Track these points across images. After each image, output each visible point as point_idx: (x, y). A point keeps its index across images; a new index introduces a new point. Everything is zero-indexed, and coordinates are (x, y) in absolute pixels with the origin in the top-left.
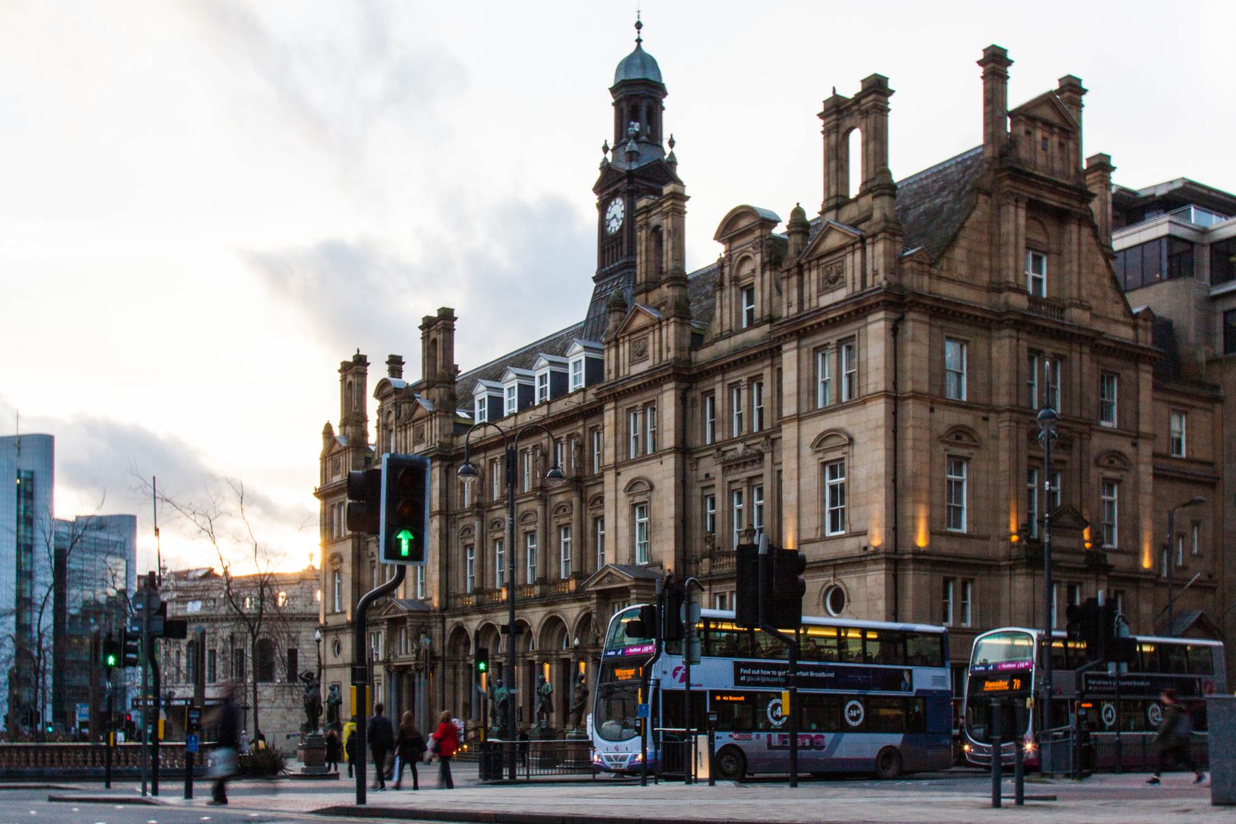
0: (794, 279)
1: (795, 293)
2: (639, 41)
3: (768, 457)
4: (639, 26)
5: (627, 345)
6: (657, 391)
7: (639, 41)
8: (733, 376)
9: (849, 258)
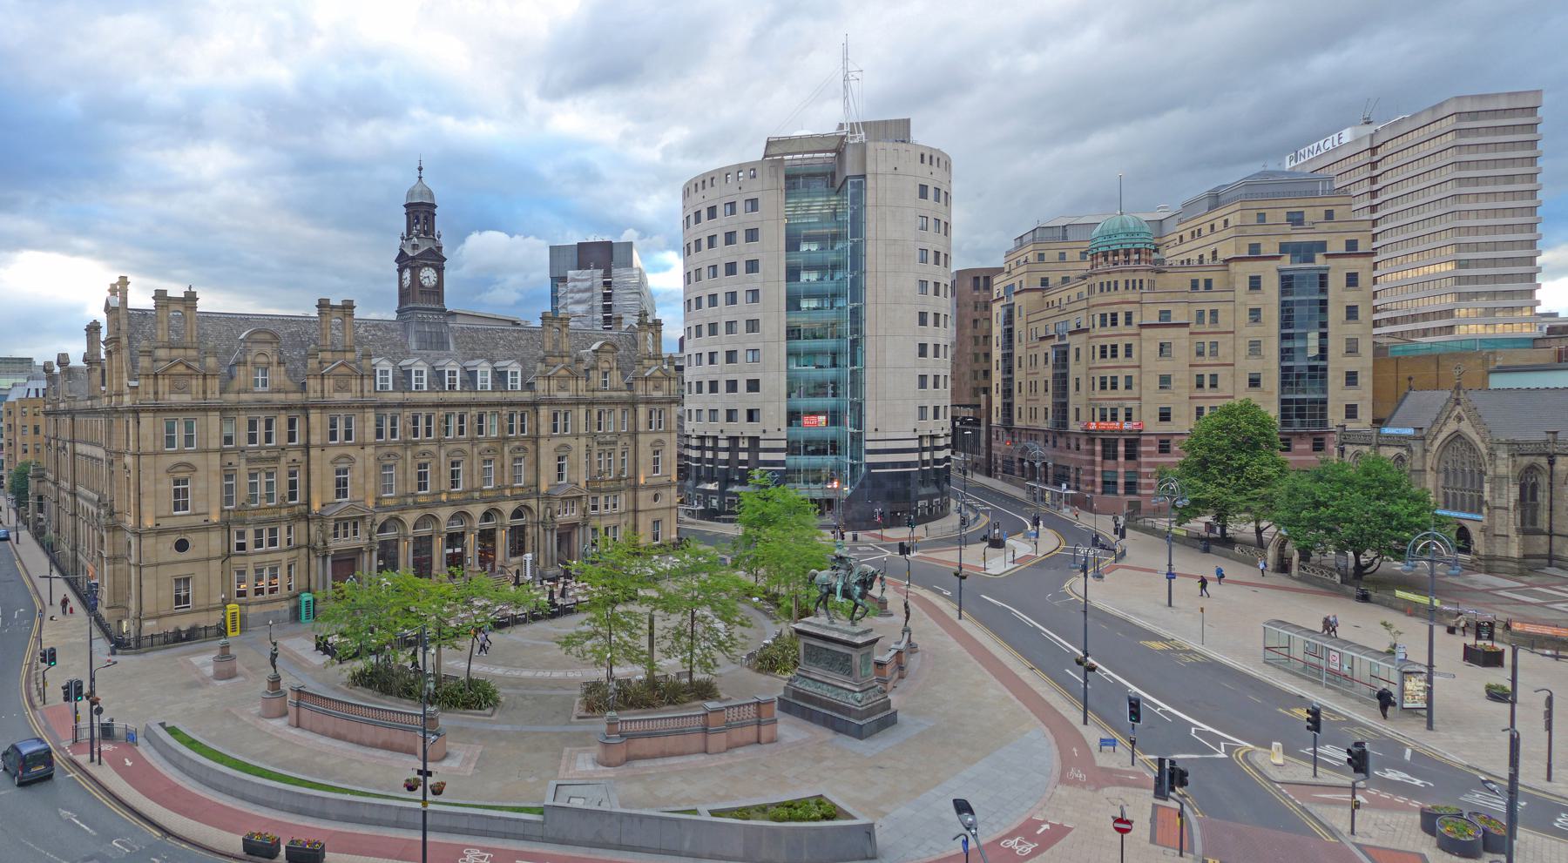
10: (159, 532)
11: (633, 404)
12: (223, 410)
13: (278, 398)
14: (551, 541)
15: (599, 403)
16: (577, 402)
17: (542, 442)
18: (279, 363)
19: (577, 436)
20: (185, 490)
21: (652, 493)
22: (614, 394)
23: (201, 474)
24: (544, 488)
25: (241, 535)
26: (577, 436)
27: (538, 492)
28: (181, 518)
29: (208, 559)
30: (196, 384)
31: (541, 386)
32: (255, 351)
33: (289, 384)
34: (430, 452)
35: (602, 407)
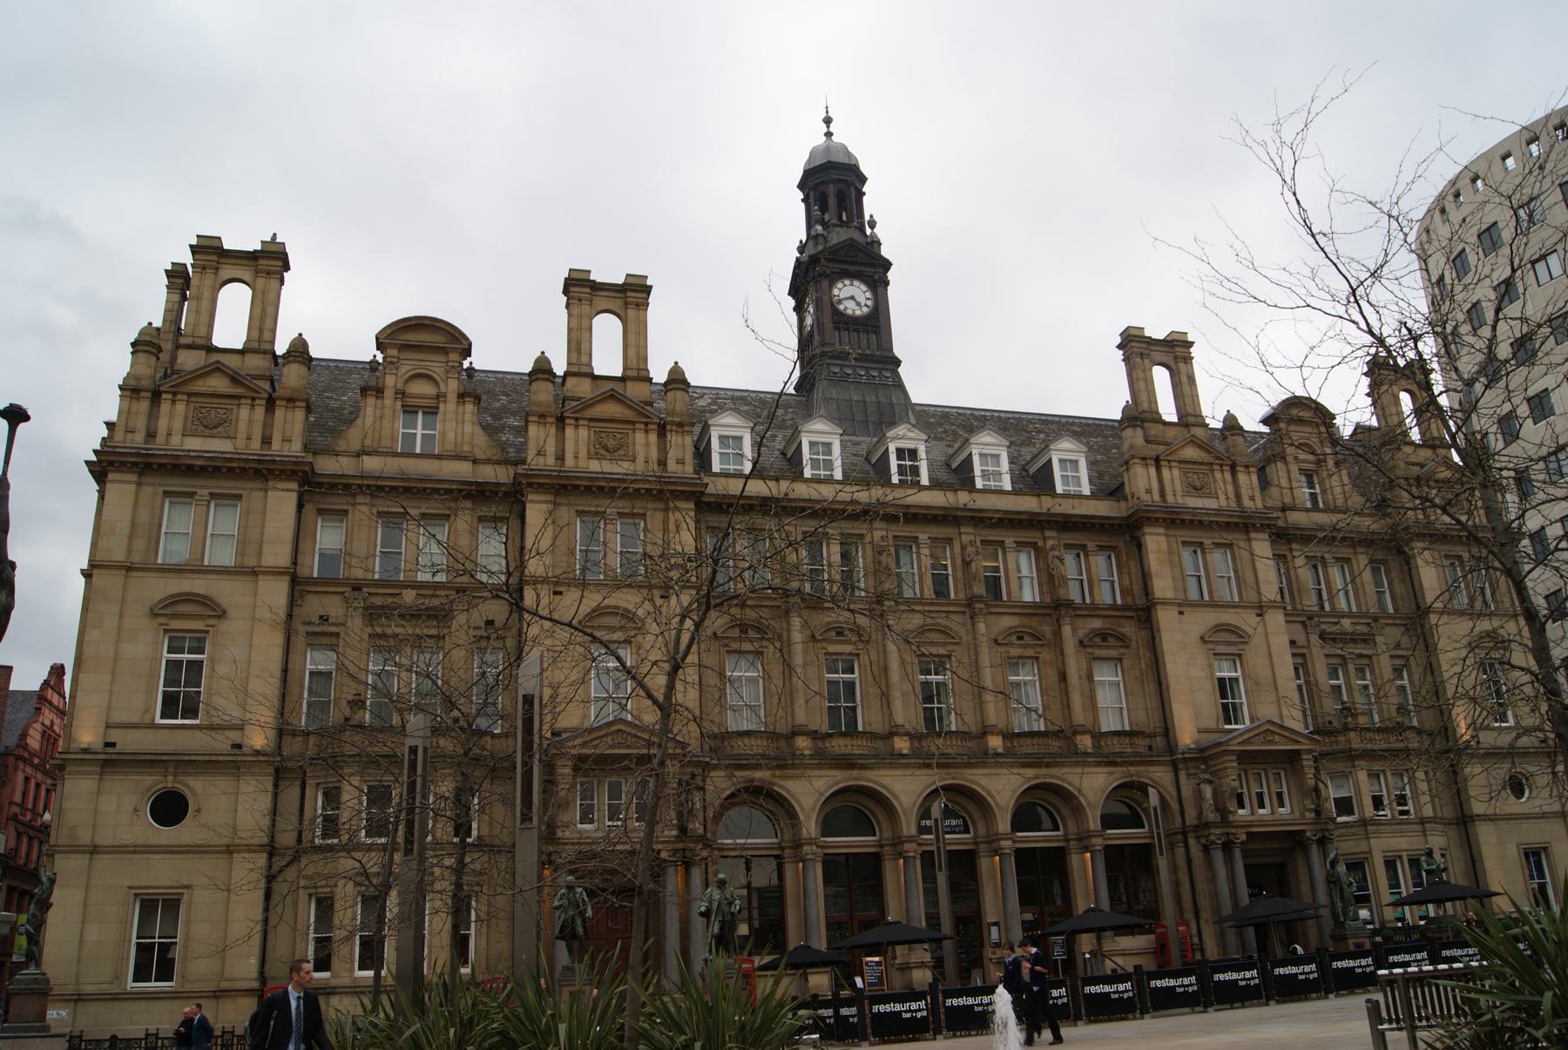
5: (1176, 472)
8: (1314, 550)
10: (110, 761)
14: (1228, 883)
17: (1165, 618)
18: (462, 397)
19: (1261, 609)
21: (1502, 770)
23: (234, 627)
24: (1186, 735)
25: (332, 797)
27: (1171, 747)
28: (181, 736)
29: (229, 850)
30: (248, 417)
32: (406, 369)
33: (480, 443)
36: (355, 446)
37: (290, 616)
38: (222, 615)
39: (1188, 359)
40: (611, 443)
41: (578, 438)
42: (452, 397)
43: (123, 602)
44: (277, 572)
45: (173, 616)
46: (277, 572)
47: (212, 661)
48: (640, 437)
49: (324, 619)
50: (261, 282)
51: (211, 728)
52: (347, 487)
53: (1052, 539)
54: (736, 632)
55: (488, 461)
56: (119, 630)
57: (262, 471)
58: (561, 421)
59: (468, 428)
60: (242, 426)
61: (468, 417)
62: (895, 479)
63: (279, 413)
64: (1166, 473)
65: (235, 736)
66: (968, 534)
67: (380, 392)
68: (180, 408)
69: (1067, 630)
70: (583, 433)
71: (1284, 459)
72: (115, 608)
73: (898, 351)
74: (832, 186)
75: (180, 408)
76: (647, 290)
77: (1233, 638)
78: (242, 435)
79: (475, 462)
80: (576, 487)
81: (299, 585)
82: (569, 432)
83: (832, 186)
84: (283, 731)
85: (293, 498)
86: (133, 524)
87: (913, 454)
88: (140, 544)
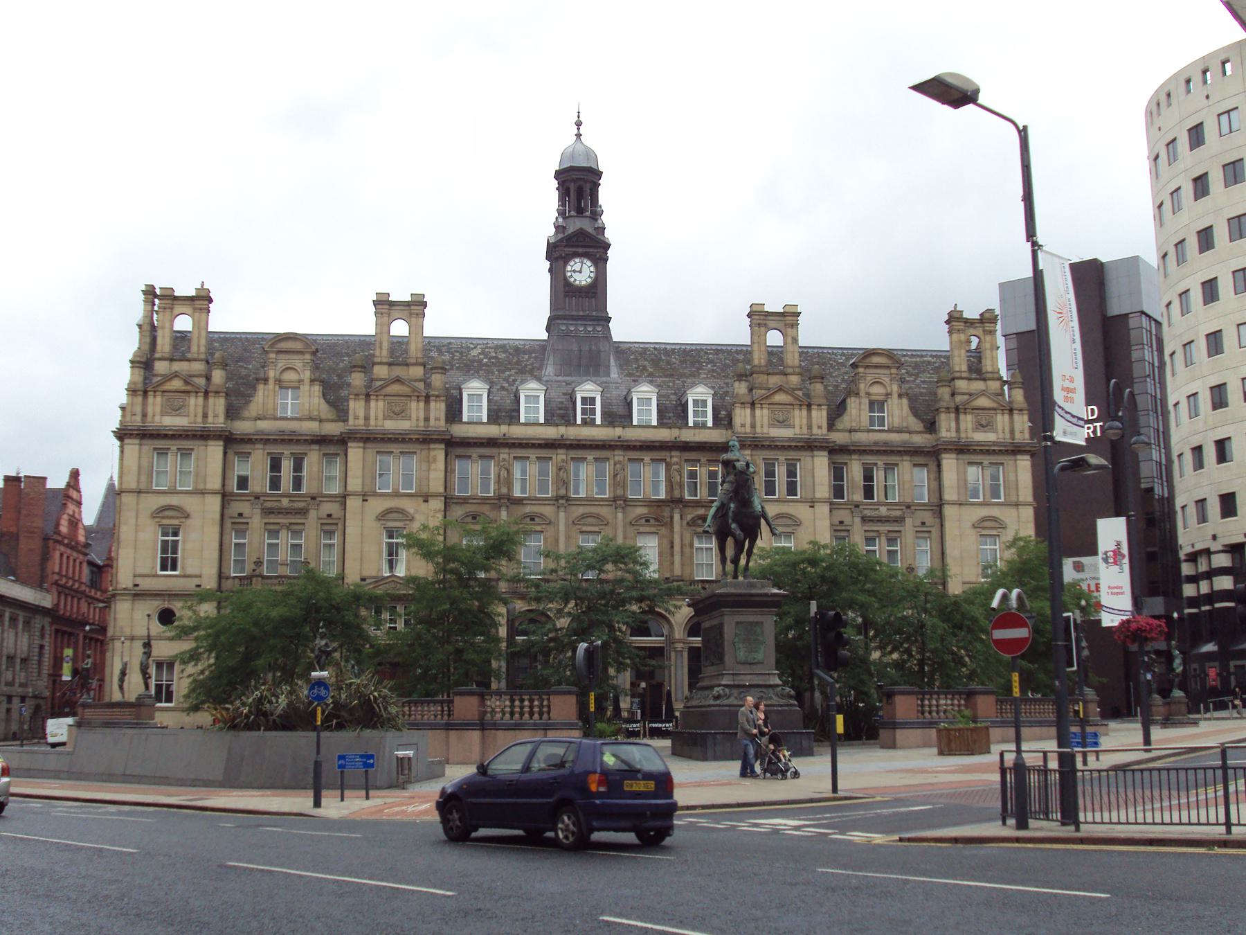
0: (953, 415)
1: (953, 424)
2: (579, 135)
3: (909, 521)
4: (579, 124)
5: (765, 411)
6: (808, 453)
7: (579, 135)
9: (999, 417)
10: (138, 595)
11: (931, 456)
12: (230, 441)
13: (311, 427)
15: (861, 451)
16: (810, 446)
18: (312, 381)
19: (812, 503)
20: (175, 543)
22: (894, 437)
26: (812, 503)
30: (195, 403)
31: (742, 417)
32: (281, 364)
34: (541, 516)
35: (870, 459)
36: (254, 414)
37: (222, 515)
38: (188, 516)
39: (795, 325)
40: (397, 409)
41: (378, 407)
42: (307, 381)
43: (137, 511)
44: (214, 493)
45: (163, 518)
46: (214, 493)
47: (184, 542)
48: (414, 405)
49: (241, 515)
50: (197, 315)
51: (185, 576)
52: (250, 440)
53: (676, 457)
54: (469, 519)
55: (328, 420)
56: (137, 525)
57: (204, 436)
58: (368, 396)
59: (316, 400)
60: (192, 409)
61: (317, 394)
62: (579, 421)
63: (211, 400)
64: (758, 412)
65: (197, 581)
66: (619, 456)
67: (266, 380)
68: (159, 399)
69: (677, 517)
70: (381, 404)
71: (857, 394)
72: (134, 514)
73: (611, 310)
74: (579, 185)
75: (159, 399)
76: (425, 305)
77: (788, 522)
78: (192, 415)
79: (321, 421)
80: (375, 438)
81: (225, 496)
82: (373, 403)
83: (579, 185)
84: (221, 576)
85: (221, 448)
86: (139, 467)
87: (593, 400)
88: (143, 478)
